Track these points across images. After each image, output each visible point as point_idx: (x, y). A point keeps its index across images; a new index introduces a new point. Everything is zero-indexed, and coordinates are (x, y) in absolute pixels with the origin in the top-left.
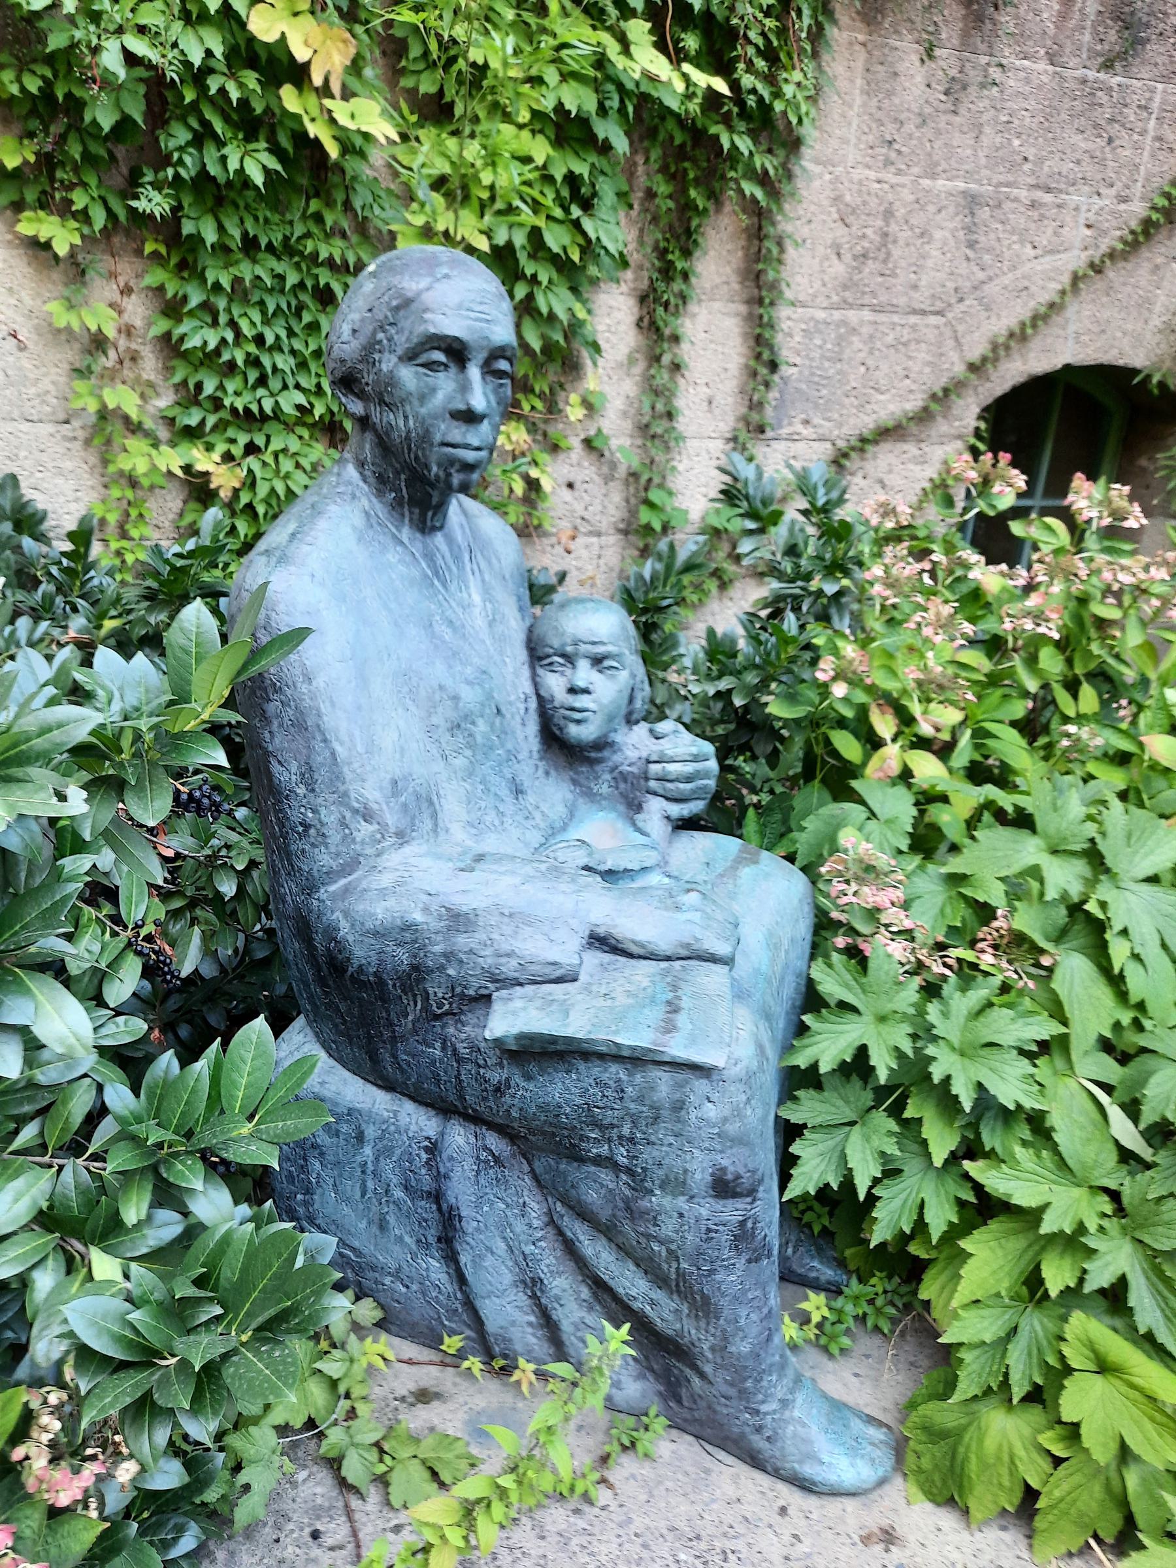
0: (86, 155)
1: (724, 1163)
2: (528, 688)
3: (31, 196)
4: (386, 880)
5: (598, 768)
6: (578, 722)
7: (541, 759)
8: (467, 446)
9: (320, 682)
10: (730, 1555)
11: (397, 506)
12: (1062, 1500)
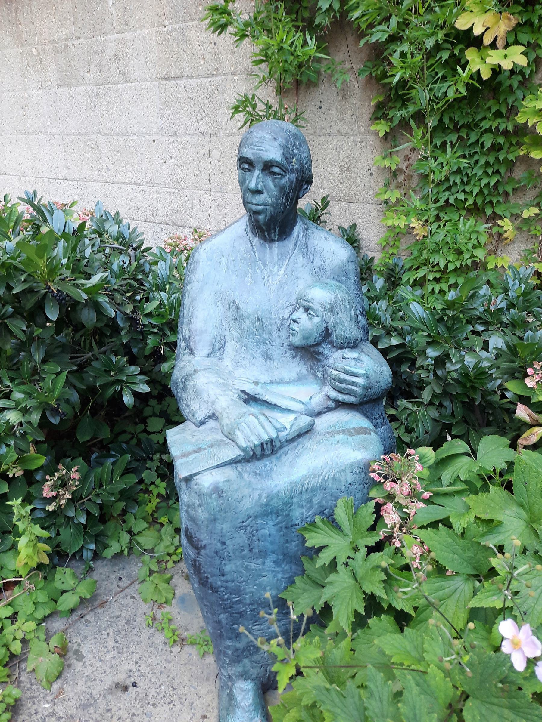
5: (320, 364)
7: (291, 350)
8: (252, 203)
10: (172, 704)
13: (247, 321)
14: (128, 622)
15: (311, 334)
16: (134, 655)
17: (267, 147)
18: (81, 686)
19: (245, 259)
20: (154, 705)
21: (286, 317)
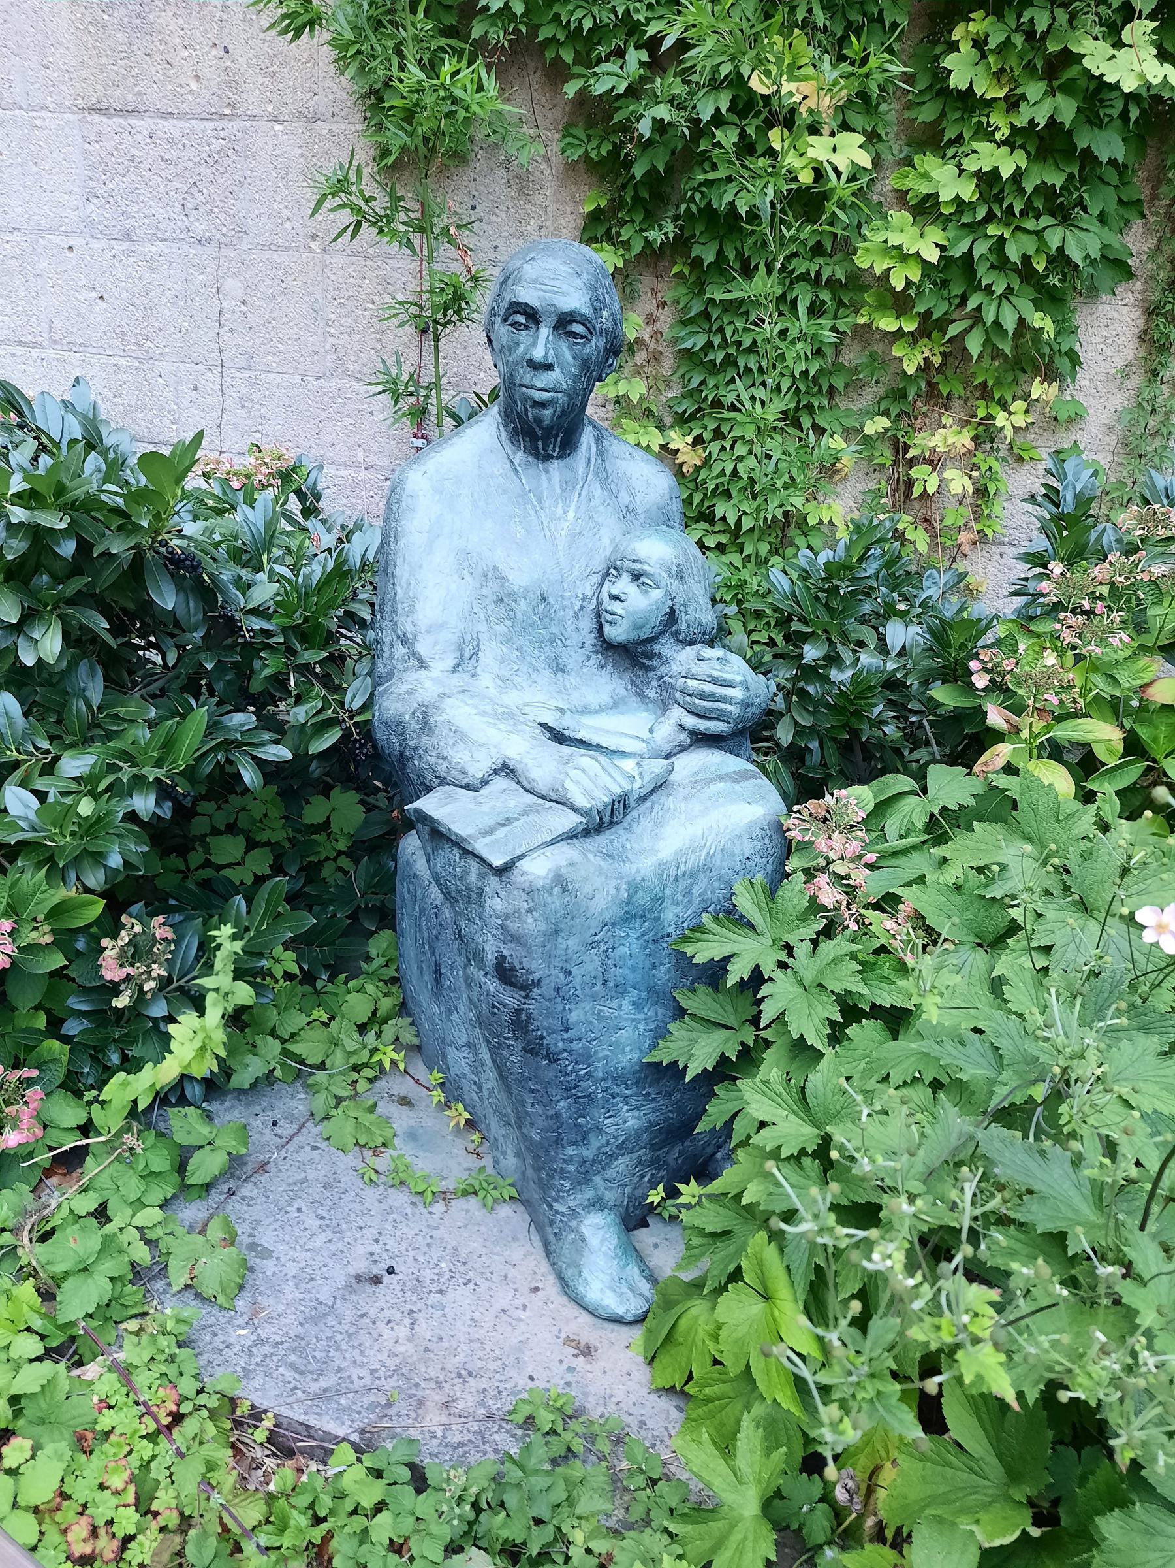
1: (506, 952)
2: (588, 589)
4: (403, 688)
5: (650, 675)
6: (610, 623)
7: (597, 653)
8: (533, 387)
9: (401, 543)
11: (514, 435)
12: (708, 1400)
13: (522, 602)
14: (327, 1186)
15: (647, 620)
16: (366, 1231)
17: (565, 288)
18: (290, 1292)
19: (505, 492)
20: (440, 1292)
21: (590, 594)
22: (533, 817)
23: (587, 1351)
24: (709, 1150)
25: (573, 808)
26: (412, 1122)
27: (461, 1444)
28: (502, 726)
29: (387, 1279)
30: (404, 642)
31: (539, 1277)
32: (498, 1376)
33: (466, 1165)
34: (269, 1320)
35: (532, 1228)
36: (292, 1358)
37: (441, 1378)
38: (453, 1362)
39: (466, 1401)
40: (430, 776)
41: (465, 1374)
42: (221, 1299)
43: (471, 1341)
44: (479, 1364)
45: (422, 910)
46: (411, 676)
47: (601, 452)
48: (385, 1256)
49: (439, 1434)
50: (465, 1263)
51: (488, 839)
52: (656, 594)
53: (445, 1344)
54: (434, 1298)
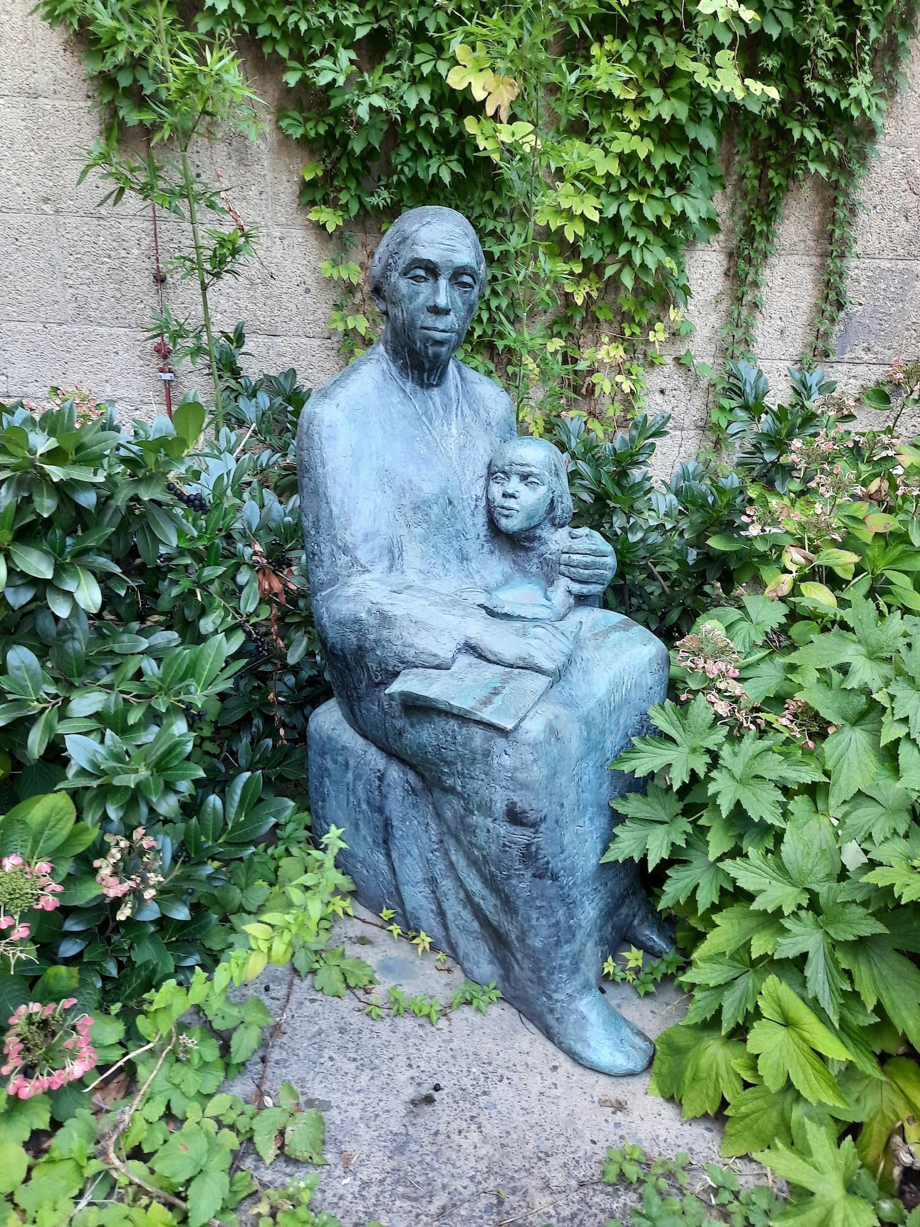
0: (350, 170)
1: (516, 799)
2: (479, 491)
3: (318, 197)
4: (351, 591)
5: (531, 554)
6: (507, 516)
7: (487, 541)
8: (435, 329)
9: (329, 467)
10: (505, 1080)
11: (403, 369)
12: (747, 1115)
13: (435, 507)
14: (342, 1031)
15: (537, 510)
16: (397, 1060)
17: (459, 246)
18: (366, 1134)
19: (405, 417)
20: (485, 1093)
21: (480, 494)
22: (513, 684)
23: (619, 1107)
24: (629, 920)
25: (539, 670)
26: (380, 957)
27: (574, 1216)
28: (455, 612)
29: (437, 1095)
30: (345, 551)
31: (551, 1057)
32: (568, 1149)
33: (443, 982)
34: (361, 1163)
35: (524, 1019)
36: (401, 1189)
37: (528, 1166)
38: (529, 1149)
39: (558, 1179)
40: (393, 662)
41: (544, 1156)
42: (316, 1159)
43: (532, 1127)
44: (549, 1144)
45: (358, 777)
46: (357, 580)
47: (463, 379)
48: (424, 1077)
49: (553, 1213)
50: (490, 1064)
51: (490, 708)
52: (543, 489)
53: (515, 1136)
54: (483, 1100)
